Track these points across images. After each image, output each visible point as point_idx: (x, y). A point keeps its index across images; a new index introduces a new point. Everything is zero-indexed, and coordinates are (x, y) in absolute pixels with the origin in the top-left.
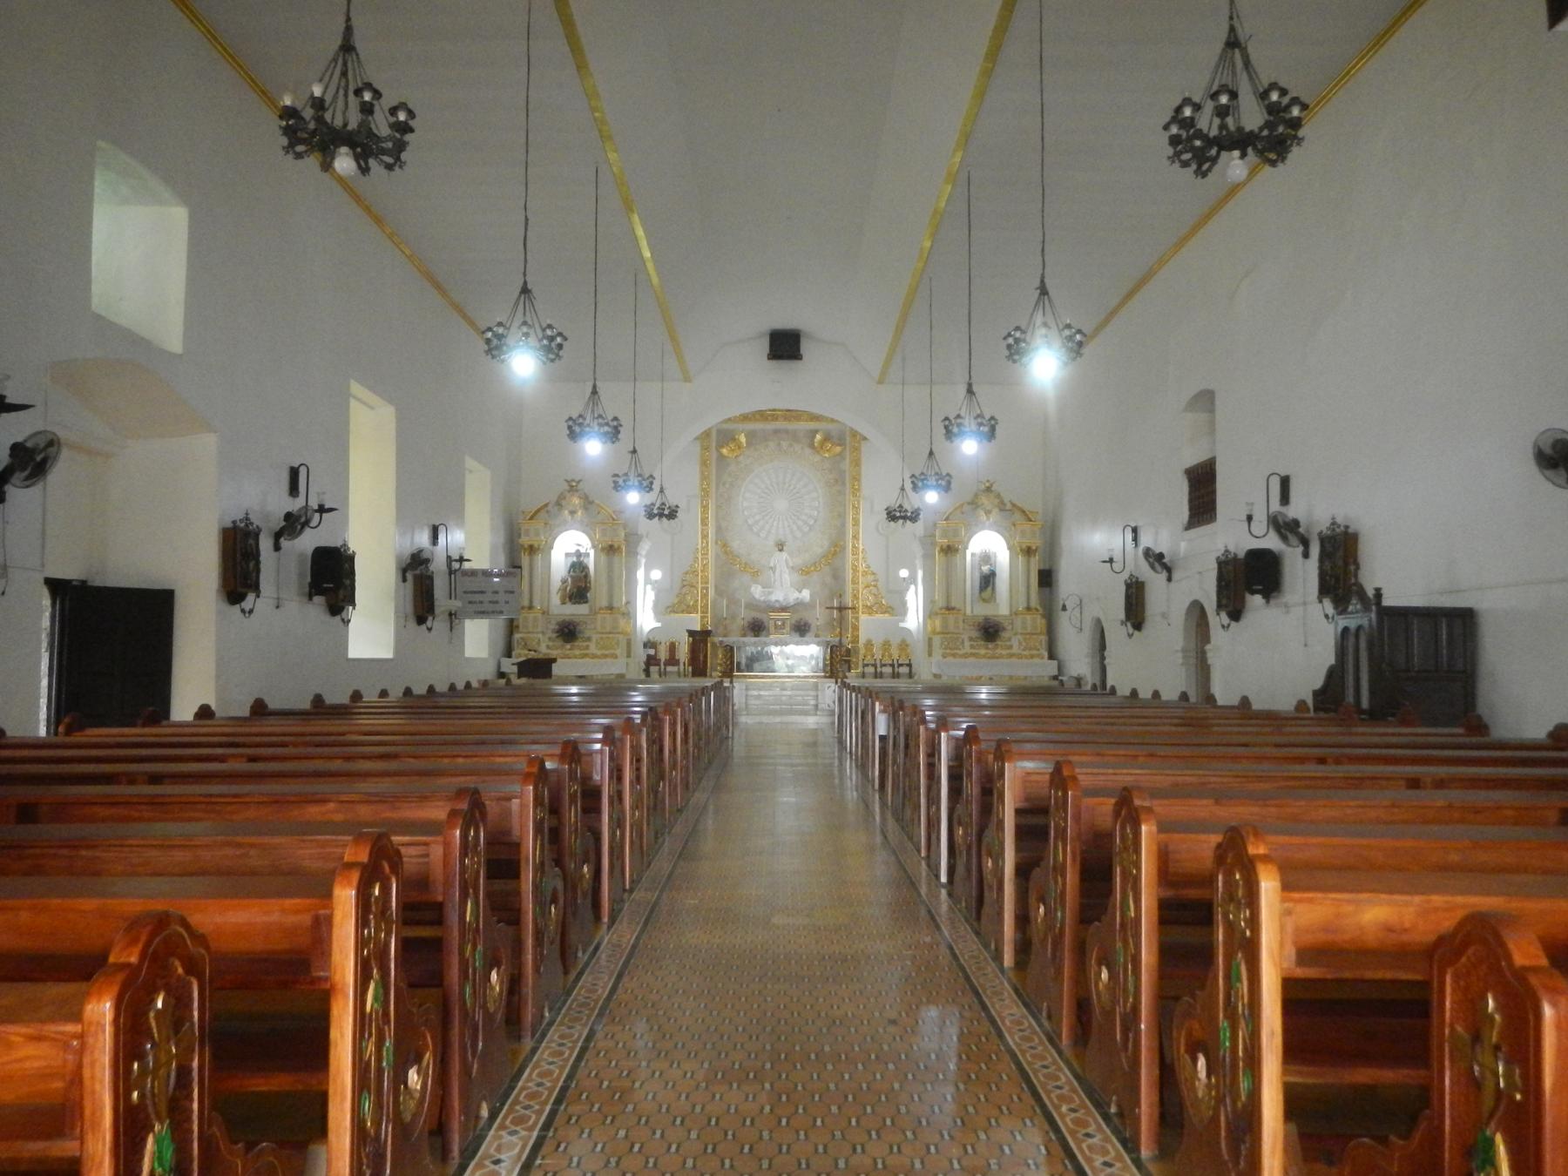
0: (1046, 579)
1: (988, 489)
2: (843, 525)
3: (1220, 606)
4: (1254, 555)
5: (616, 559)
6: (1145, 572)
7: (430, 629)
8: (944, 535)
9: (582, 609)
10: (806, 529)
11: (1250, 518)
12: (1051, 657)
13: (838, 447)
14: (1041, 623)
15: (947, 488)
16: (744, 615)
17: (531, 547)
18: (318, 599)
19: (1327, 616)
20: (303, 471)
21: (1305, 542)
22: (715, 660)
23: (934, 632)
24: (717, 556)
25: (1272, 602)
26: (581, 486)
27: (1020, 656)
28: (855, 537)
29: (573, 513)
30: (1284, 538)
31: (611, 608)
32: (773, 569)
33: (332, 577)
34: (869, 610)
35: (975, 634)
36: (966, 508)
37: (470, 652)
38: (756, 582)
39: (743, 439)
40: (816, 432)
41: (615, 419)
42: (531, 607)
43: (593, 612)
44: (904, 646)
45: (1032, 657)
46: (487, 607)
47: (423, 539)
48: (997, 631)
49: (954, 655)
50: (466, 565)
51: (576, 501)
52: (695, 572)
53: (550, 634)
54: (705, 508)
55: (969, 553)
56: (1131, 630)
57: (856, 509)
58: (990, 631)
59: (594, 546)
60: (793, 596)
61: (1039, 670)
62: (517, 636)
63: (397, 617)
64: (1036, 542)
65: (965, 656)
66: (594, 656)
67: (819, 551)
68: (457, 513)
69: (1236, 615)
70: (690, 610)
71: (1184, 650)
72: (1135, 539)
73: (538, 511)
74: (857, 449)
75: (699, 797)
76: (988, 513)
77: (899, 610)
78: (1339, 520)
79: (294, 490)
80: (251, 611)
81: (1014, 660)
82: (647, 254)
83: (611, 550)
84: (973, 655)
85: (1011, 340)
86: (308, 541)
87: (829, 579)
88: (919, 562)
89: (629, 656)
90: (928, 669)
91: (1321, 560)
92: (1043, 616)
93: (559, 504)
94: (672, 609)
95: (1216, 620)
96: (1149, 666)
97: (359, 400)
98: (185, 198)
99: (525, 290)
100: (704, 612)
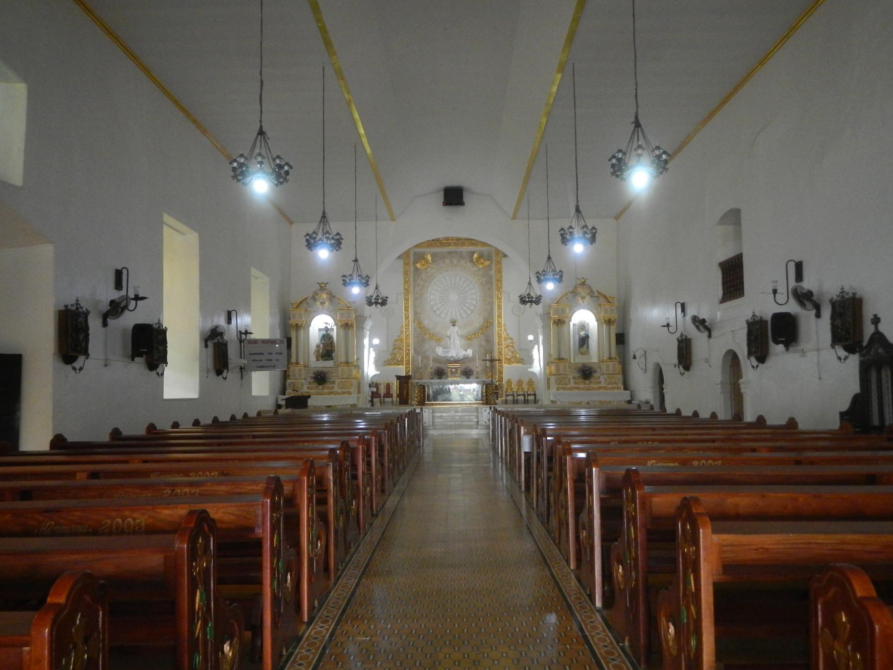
0: (621, 339)
1: (583, 284)
2: (492, 309)
3: (750, 354)
4: (777, 317)
5: (350, 332)
6: (692, 331)
7: (225, 379)
8: (556, 313)
9: (329, 364)
10: (469, 312)
11: (775, 292)
12: (626, 388)
13: (488, 260)
14: (618, 367)
15: (560, 280)
16: (432, 366)
17: (297, 325)
18: (137, 359)
19: (839, 358)
20: (125, 271)
21: (818, 307)
22: (415, 394)
23: (551, 374)
24: (415, 330)
25: (791, 349)
26: (328, 286)
27: (605, 388)
28: (499, 316)
29: (322, 303)
30: (802, 304)
31: (347, 363)
32: (449, 337)
33: (149, 345)
34: (509, 361)
35: (577, 375)
36: (570, 295)
37: (255, 392)
38: (439, 345)
39: (429, 258)
40: (473, 253)
41: (338, 234)
42: (297, 363)
43: (337, 366)
44: (531, 383)
45: (614, 388)
46: (264, 363)
47: (221, 321)
48: (591, 373)
49: (564, 389)
50: (253, 337)
51: (325, 296)
52: (401, 340)
53: (309, 379)
54: (407, 300)
55: (571, 323)
56: (682, 370)
57: (499, 299)
58: (586, 373)
59: (336, 324)
60: (462, 353)
61: (617, 397)
62: (288, 381)
63: (201, 371)
64: (614, 316)
65: (572, 389)
66: (337, 393)
68: (247, 307)
69: (762, 359)
70: (399, 363)
71: (722, 383)
72: (683, 310)
73: (301, 303)
74: (499, 263)
75: (392, 501)
76: (583, 298)
77: (530, 361)
78: (846, 289)
79: (118, 285)
80: (81, 369)
81: (602, 390)
82: (362, 131)
83: (346, 326)
84: (576, 388)
85: (614, 161)
86: (130, 319)
87: (483, 343)
88: (540, 330)
89: (359, 392)
90: (548, 397)
91: (833, 318)
92: (620, 363)
93: (314, 299)
94: (388, 363)
95: (747, 363)
96: (697, 394)
97: (170, 226)
98: (25, 79)
99: (261, 133)
100: (408, 364)
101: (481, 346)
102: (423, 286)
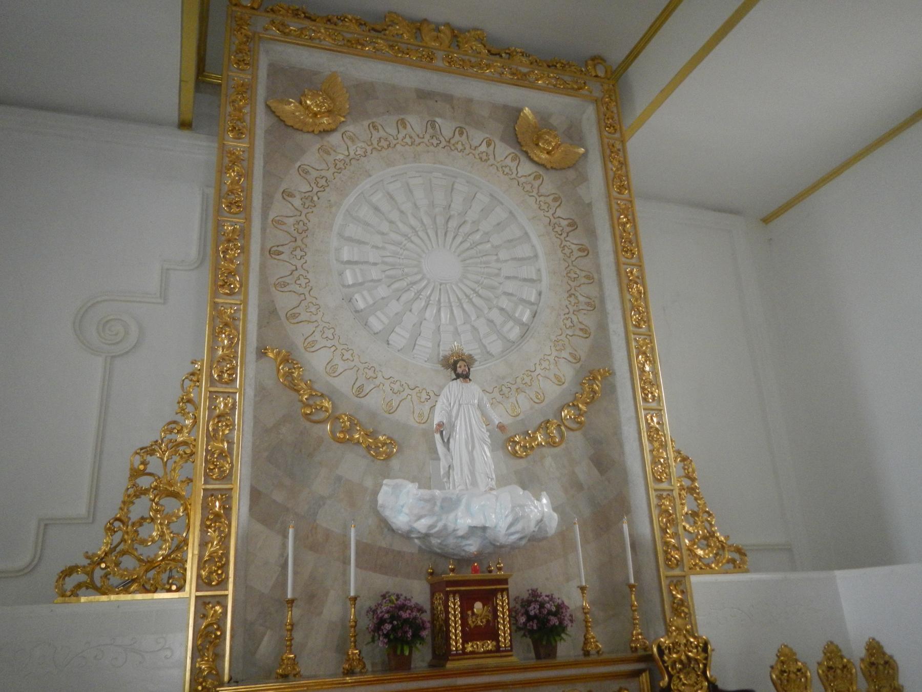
2: (603, 327)
10: (514, 333)
24: (262, 394)
67: (552, 391)
87: (585, 471)
101: (578, 486)
102: (309, 201)
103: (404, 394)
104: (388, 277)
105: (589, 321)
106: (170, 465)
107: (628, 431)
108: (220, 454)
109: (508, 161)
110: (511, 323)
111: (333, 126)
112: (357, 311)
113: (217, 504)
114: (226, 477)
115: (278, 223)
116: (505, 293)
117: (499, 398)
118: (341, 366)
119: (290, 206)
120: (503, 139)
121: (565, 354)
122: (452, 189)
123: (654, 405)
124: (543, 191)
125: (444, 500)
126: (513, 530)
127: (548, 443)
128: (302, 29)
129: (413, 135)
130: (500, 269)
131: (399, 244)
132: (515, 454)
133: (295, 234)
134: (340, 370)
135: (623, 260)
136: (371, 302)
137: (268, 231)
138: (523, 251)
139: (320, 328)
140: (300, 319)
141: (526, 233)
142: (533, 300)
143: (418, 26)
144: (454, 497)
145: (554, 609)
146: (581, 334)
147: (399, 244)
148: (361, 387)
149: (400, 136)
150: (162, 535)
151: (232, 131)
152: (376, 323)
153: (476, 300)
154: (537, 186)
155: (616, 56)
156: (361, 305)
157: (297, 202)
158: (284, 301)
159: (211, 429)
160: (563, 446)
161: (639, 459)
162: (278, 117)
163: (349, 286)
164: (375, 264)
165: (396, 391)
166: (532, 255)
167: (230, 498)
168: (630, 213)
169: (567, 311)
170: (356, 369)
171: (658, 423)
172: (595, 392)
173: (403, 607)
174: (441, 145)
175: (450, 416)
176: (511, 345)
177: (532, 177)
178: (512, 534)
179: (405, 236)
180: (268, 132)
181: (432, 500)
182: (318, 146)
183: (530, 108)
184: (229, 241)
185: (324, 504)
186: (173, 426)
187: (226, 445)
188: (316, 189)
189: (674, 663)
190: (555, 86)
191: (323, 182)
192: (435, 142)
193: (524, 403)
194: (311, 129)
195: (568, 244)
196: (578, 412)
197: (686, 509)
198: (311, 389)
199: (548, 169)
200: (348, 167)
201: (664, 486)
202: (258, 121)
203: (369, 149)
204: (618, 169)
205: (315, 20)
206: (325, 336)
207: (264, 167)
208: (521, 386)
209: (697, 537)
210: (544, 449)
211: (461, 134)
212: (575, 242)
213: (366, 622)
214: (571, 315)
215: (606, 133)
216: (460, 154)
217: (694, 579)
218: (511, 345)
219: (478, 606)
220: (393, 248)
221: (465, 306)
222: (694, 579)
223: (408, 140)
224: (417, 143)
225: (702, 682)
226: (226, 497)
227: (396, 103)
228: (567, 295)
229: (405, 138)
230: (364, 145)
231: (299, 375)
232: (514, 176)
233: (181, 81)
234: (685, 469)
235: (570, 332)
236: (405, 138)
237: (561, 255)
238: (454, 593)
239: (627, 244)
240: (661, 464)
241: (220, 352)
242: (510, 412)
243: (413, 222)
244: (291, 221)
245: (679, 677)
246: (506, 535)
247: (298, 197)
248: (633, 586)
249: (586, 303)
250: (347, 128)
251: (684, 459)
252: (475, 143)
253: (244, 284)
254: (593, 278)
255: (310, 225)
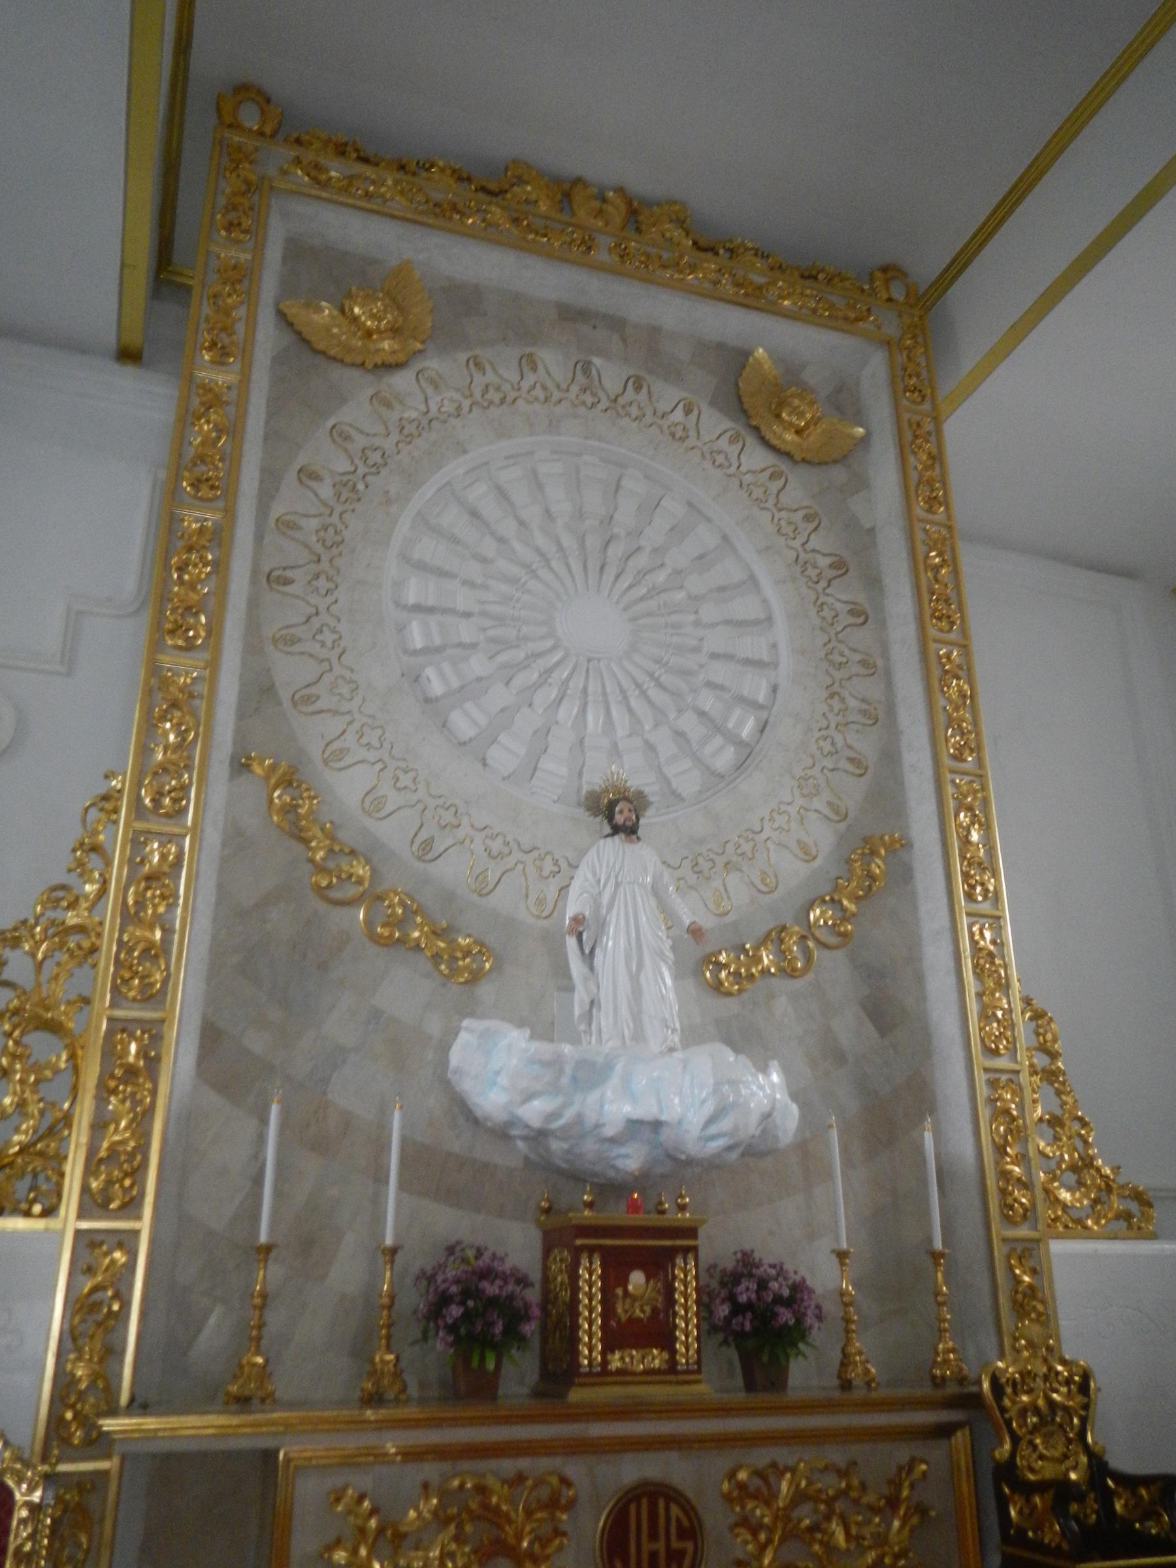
2: (891, 756)
10: (725, 759)
24: (236, 841)
67: (793, 872)
87: (849, 1027)
102: (347, 488)
103: (510, 862)
104: (493, 640)
105: (867, 745)
106: (49, 968)
107: (936, 956)
108: (145, 952)
109: (723, 443)
110: (718, 741)
111: (401, 357)
112: (428, 700)
113: (133, 1047)
114: (152, 997)
115: (287, 526)
116: (710, 685)
117: (692, 878)
118: (393, 800)
119: (311, 495)
120: (713, 403)
121: (818, 803)
122: (618, 487)
123: (986, 908)
124: (785, 499)
125: (581, 1064)
126: (713, 1130)
127: (781, 970)
128: (351, 178)
129: (549, 384)
130: (701, 640)
131: (513, 581)
132: (717, 987)
133: (319, 548)
134: (389, 808)
135: (932, 632)
136: (455, 683)
137: (266, 540)
138: (745, 607)
139: (356, 725)
140: (319, 705)
141: (752, 578)
142: (761, 698)
143: (567, 191)
144: (600, 1059)
145: (786, 1292)
146: (850, 767)
147: (513, 581)
148: (428, 844)
149: (525, 385)
150: (21, 1105)
151: (209, 349)
152: (463, 724)
153: (653, 693)
154: (775, 492)
155: (926, 266)
156: (437, 688)
157: (325, 490)
158: (291, 672)
159: (131, 901)
160: (810, 976)
161: (954, 1009)
162: (299, 333)
163: (415, 653)
164: (467, 615)
165: (495, 852)
166: (762, 616)
167: (157, 1039)
168: (948, 549)
169: (824, 724)
170: (420, 807)
171: (994, 942)
172: (872, 878)
173: (486, 1274)
174: (602, 406)
175: (597, 905)
176: (716, 780)
177: (767, 473)
178: (713, 1138)
179: (527, 567)
180: (278, 360)
181: (555, 1064)
182: (371, 391)
183: (765, 350)
184: (190, 549)
185: (344, 1062)
186: (60, 895)
187: (158, 935)
188: (362, 469)
189: (1023, 1412)
190: (814, 311)
191: (376, 457)
192: (589, 400)
193: (738, 891)
194: (359, 360)
195: (830, 600)
196: (840, 914)
197: (1039, 1111)
198: (333, 839)
199: (796, 462)
200: (424, 434)
201: (1002, 1063)
202: (261, 335)
203: (466, 404)
204: (926, 468)
205: (377, 165)
206: (364, 741)
207: (267, 423)
208: (734, 858)
209: (1059, 1167)
210: (773, 980)
211: (638, 388)
212: (843, 597)
213: (414, 1300)
214: (831, 731)
215: (905, 402)
216: (635, 424)
217: (1057, 1247)
218: (716, 780)
219: (637, 1279)
220: (504, 588)
221: (633, 702)
222: (1057, 1247)
223: (539, 392)
224: (554, 399)
225: (1076, 1453)
226: (154, 1034)
227: (522, 325)
228: (825, 694)
229: (533, 387)
230: (457, 396)
231: (311, 811)
232: (733, 470)
233: (123, 265)
234: (1038, 1034)
235: (828, 763)
236: (533, 387)
237: (817, 621)
238: (591, 1250)
239: (941, 605)
240: (998, 1021)
241: (160, 756)
242: (711, 906)
243: (541, 541)
244: (314, 523)
245: (1031, 1443)
246: (700, 1139)
247: (328, 481)
248: (942, 1255)
249: (860, 711)
250: (427, 363)
251: (1038, 1015)
252: (664, 406)
253: (214, 631)
254: (875, 666)
255: (347, 534)
